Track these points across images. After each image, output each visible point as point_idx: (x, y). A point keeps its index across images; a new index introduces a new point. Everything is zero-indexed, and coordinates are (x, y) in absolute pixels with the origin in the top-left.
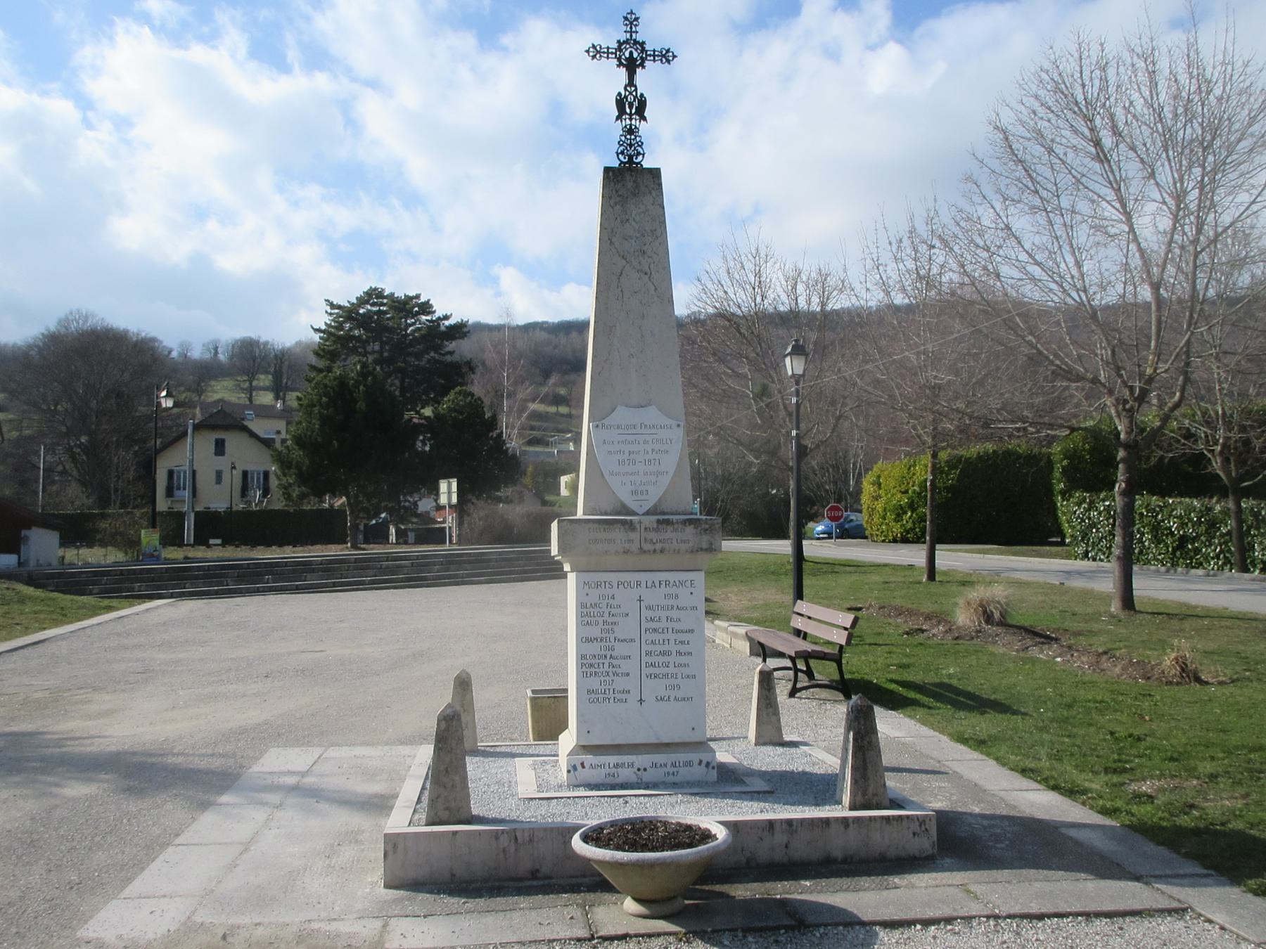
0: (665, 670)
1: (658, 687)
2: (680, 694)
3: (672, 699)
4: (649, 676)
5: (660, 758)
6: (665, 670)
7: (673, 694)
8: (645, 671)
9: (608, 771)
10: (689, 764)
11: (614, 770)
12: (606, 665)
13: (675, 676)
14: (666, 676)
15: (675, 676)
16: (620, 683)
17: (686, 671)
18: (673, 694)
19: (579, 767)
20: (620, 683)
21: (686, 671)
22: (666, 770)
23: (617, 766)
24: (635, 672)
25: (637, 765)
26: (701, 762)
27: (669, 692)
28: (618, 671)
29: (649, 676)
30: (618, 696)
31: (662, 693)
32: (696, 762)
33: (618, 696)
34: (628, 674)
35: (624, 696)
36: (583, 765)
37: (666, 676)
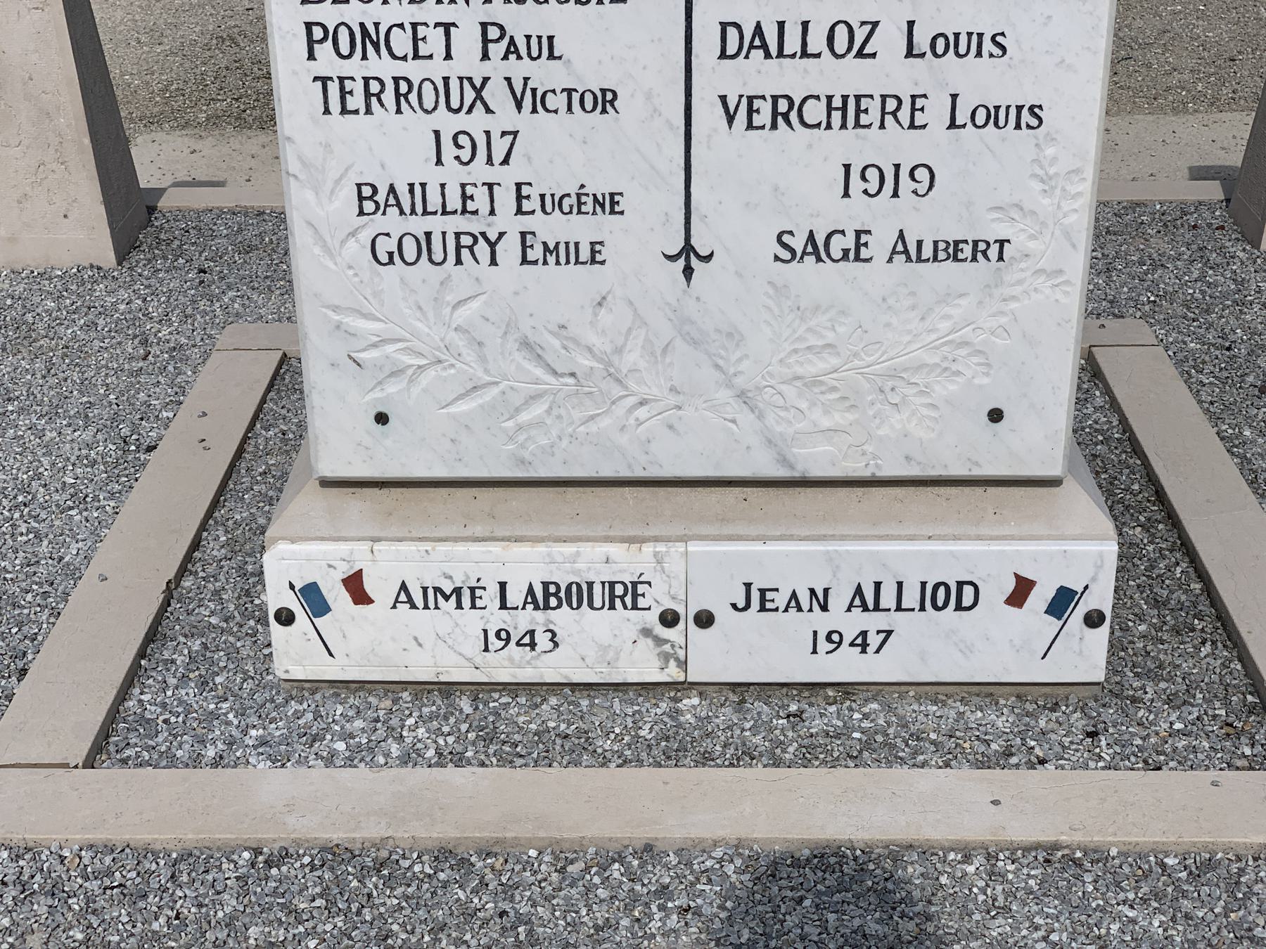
0: (846, 77)
1: (800, 175)
2: (928, 220)
3: (880, 245)
4: (740, 111)
5: (789, 561)
6: (846, 77)
7: (884, 218)
8: (716, 78)
9: (497, 619)
10: (951, 596)
11: (526, 619)
12: (467, 40)
13: (904, 110)
14: (847, 111)
15: (904, 110)
16: (556, 152)
17: (979, 81)
18: (884, 218)
19: (338, 597)
20: (556, 152)
21: (979, 81)
22: (822, 622)
23: (546, 597)
24: (649, 78)
25: (657, 598)
26: (1021, 591)
27: (857, 212)
28: (544, 74)
29: (740, 111)
30: (551, 228)
31: (831, 213)
32: (997, 588)
33: (551, 228)
34: (606, 100)
35: (580, 229)
36: (355, 587)
37: (847, 111)
